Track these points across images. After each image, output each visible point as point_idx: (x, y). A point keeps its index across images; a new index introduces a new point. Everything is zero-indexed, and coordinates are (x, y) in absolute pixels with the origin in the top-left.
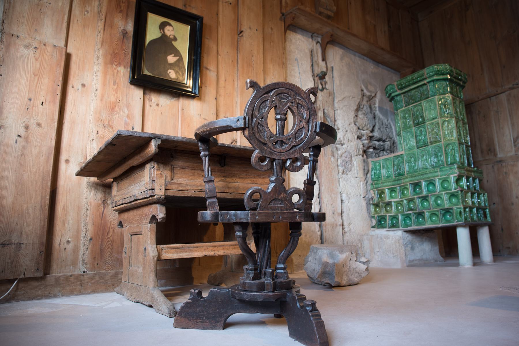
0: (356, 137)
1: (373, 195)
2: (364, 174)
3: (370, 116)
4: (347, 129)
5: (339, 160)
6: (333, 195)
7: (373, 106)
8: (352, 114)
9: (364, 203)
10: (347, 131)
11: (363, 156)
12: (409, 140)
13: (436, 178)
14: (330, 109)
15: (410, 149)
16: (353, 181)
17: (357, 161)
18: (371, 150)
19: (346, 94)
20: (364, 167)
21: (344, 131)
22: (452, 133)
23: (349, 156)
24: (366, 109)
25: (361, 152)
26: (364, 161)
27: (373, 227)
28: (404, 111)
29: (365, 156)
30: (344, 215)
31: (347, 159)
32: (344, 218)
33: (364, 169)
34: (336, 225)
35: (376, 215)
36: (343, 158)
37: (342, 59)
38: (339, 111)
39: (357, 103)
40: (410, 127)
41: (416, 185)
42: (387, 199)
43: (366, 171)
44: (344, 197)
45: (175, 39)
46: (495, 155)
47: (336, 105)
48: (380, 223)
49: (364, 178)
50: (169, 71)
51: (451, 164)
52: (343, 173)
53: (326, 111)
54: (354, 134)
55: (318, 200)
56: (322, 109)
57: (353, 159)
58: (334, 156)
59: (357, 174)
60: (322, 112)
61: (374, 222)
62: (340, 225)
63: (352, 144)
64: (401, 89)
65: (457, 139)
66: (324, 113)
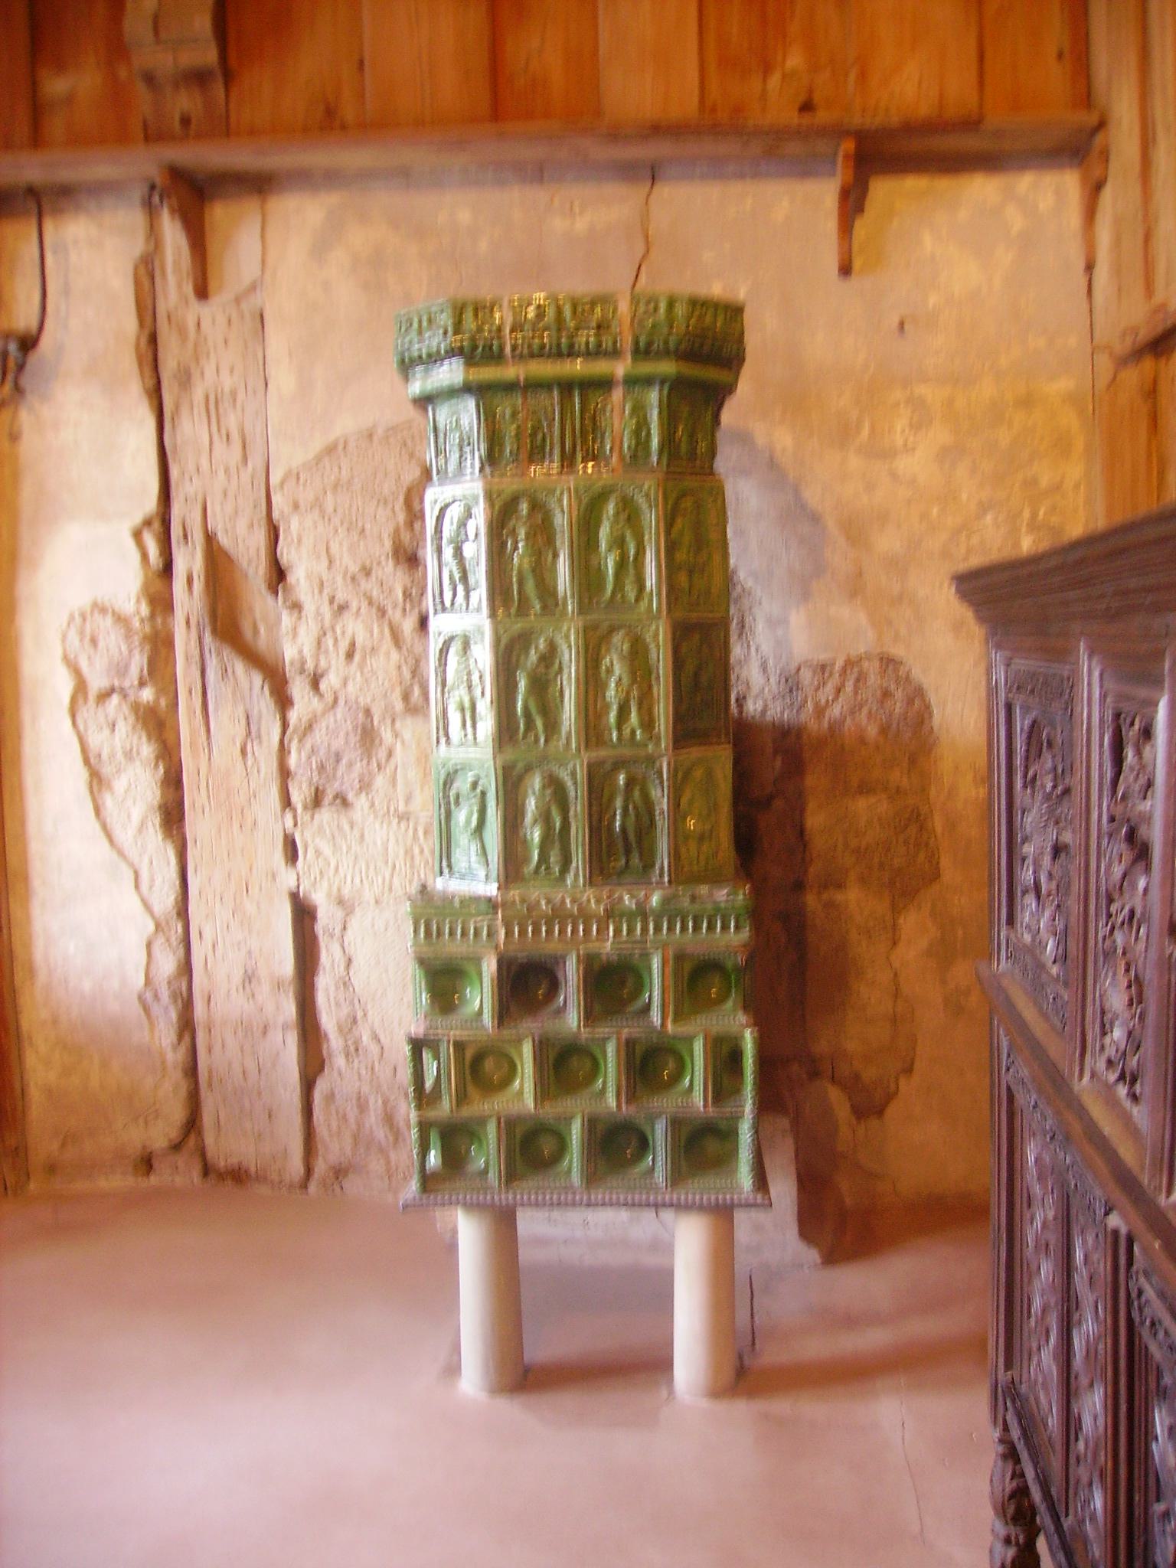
4: (341, 597)
5: (294, 747)
6: (250, 907)
10: (342, 608)
14: (242, 525)
16: (381, 834)
19: (346, 425)
21: (327, 611)
31: (338, 743)
34: (265, 1030)
36: (319, 736)
37: (320, 250)
38: (295, 524)
47: (276, 499)
52: (317, 801)
56: (198, 537)
58: (259, 737)
59: (408, 799)
62: (285, 1027)
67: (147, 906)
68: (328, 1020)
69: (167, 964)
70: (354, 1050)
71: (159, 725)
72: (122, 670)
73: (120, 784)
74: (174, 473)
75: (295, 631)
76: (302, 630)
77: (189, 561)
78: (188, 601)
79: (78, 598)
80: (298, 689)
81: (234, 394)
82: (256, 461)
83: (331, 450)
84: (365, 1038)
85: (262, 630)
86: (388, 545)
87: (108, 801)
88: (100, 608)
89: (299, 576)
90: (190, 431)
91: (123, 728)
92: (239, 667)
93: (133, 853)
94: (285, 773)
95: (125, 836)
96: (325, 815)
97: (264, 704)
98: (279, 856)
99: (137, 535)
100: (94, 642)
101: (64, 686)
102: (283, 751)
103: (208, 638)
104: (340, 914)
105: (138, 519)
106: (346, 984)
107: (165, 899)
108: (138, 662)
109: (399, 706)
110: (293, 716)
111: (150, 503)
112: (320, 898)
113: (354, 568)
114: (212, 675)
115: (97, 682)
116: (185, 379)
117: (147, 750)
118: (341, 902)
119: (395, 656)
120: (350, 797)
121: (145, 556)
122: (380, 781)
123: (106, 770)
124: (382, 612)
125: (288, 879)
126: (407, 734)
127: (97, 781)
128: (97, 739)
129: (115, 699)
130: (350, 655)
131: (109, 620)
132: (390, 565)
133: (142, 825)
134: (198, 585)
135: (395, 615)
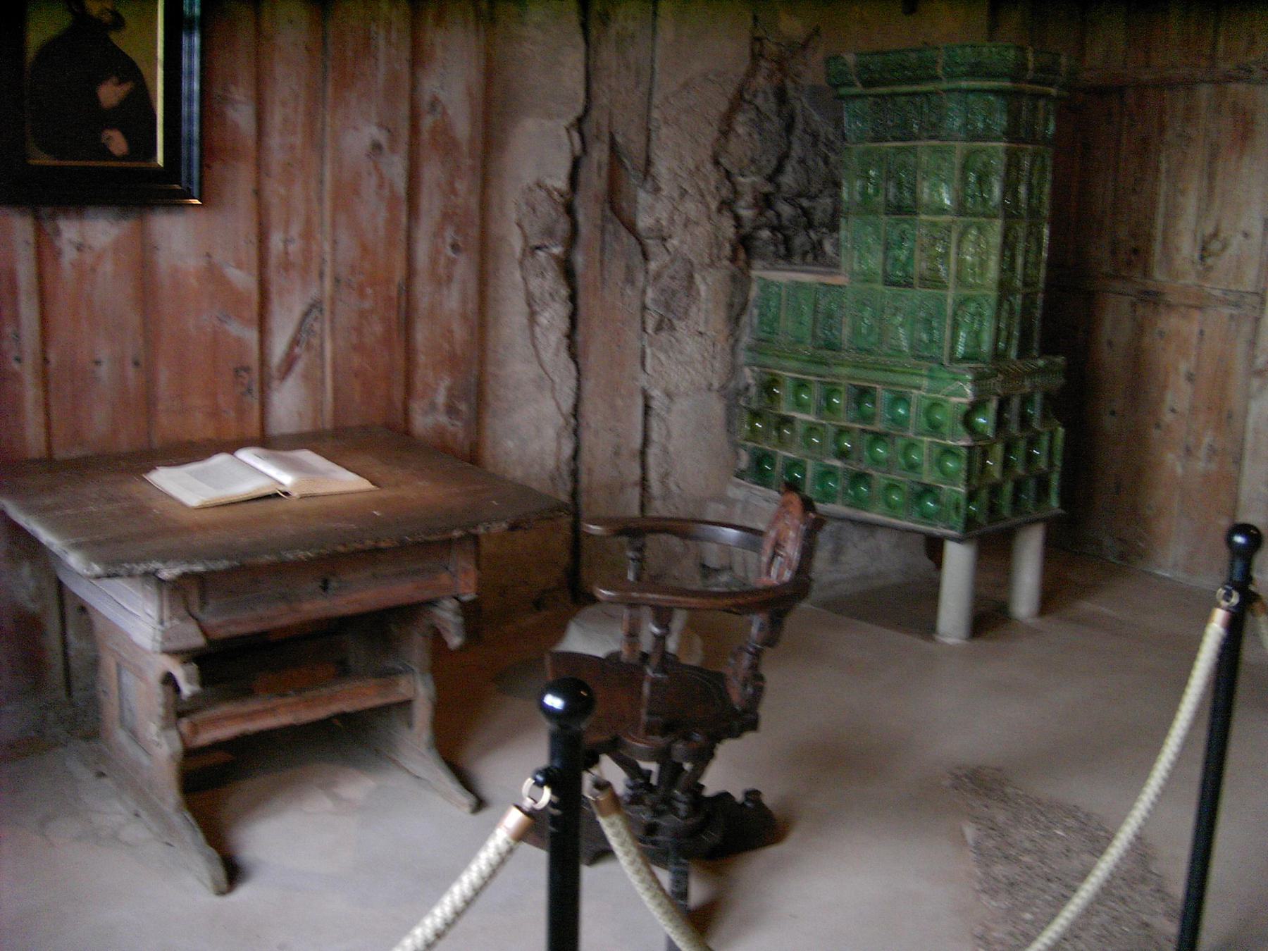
0: (714, 206)
1: (751, 381)
2: (729, 318)
3: (774, 125)
6: (619, 402)
7: (789, 84)
8: (710, 133)
9: (717, 408)
11: (733, 259)
12: (869, 250)
13: (915, 391)
15: (868, 278)
16: (691, 346)
17: (710, 285)
18: (765, 234)
20: (733, 295)
21: (676, 195)
22: (983, 264)
23: (683, 274)
24: (767, 104)
25: (727, 250)
26: (733, 278)
27: (740, 474)
28: (868, 152)
29: (742, 255)
30: (653, 451)
31: (675, 285)
32: (651, 460)
33: (731, 306)
34: (623, 487)
35: (749, 444)
36: (665, 280)
38: (664, 131)
39: (731, 90)
40: (874, 212)
41: (863, 394)
42: (784, 412)
43: (737, 308)
44: (655, 404)
45: (118, 23)
46: (1146, 273)
47: (656, 114)
48: (759, 470)
49: (726, 332)
50: (109, 133)
51: (966, 358)
52: (659, 328)
53: (619, 139)
54: (709, 199)
55: (572, 421)
56: (606, 138)
57: (697, 277)
59: (706, 322)
60: (606, 148)
61: (744, 461)
62: (636, 484)
63: (698, 231)
64: (868, 83)
65: (994, 286)
66: (613, 145)
67: (559, 408)
68: (653, 476)
69: (567, 450)
70: (667, 495)
71: (567, 271)
72: (549, 232)
73: (544, 319)
74: (595, 86)
75: (652, 207)
76: (659, 206)
77: (599, 154)
78: (594, 180)
79: (528, 175)
80: (652, 244)
81: (633, 37)
82: (643, 88)
83: (685, 86)
84: (673, 487)
85: (624, 205)
86: (710, 153)
87: (537, 329)
88: (539, 185)
89: (663, 167)
90: (607, 55)
91: (550, 275)
92: (623, 232)
93: (550, 370)
94: (644, 307)
95: (547, 356)
96: (664, 336)
97: (638, 258)
98: (639, 366)
99: (568, 130)
100: (534, 210)
101: (517, 243)
102: (644, 292)
103: (609, 213)
104: (667, 401)
105: (571, 118)
106: (665, 451)
107: (567, 405)
108: (563, 226)
109: (707, 260)
110: (653, 266)
111: (579, 109)
112: (656, 393)
113: (692, 167)
114: (608, 238)
115: (536, 242)
116: (605, 19)
117: (564, 292)
118: (669, 395)
119: (708, 227)
120: (675, 322)
121: (572, 144)
122: (694, 309)
123: (537, 308)
124: (703, 196)
125: (643, 381)
126: (709, 280)
127: (532, 316)
128: (535, 283)
129: (540, 253)
130: (686, 226)
131: (544, 194)
132: (709, 166)
133: (558, 350)
134: (604, 173)
135: (709, 199)
